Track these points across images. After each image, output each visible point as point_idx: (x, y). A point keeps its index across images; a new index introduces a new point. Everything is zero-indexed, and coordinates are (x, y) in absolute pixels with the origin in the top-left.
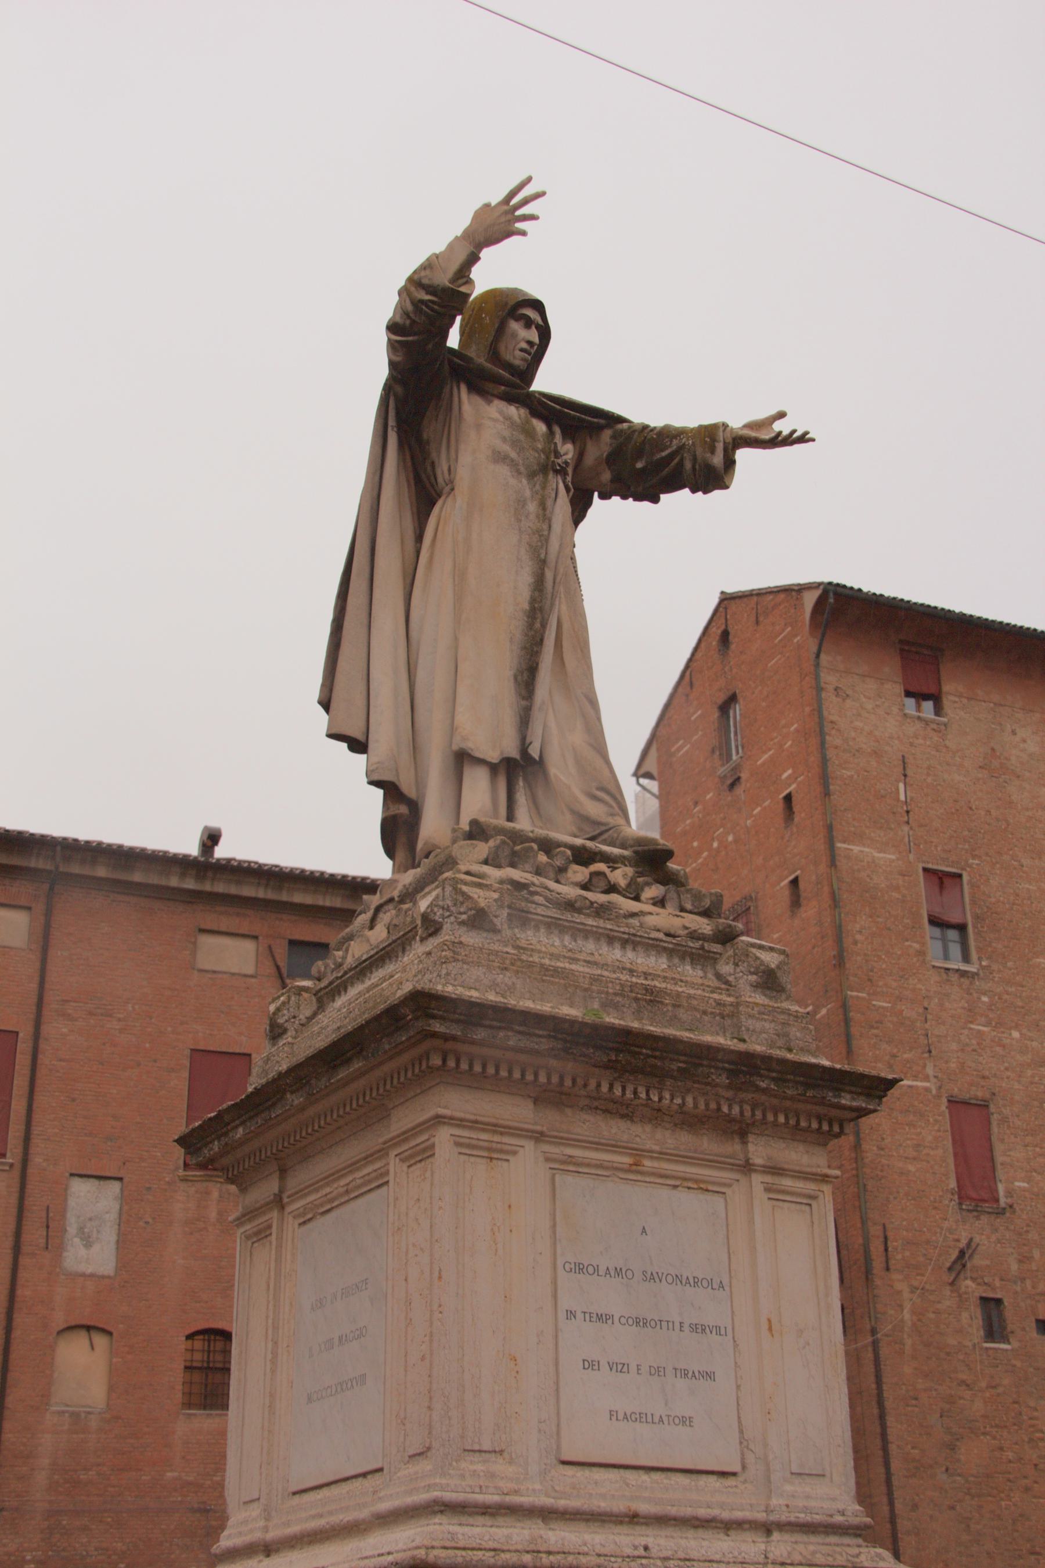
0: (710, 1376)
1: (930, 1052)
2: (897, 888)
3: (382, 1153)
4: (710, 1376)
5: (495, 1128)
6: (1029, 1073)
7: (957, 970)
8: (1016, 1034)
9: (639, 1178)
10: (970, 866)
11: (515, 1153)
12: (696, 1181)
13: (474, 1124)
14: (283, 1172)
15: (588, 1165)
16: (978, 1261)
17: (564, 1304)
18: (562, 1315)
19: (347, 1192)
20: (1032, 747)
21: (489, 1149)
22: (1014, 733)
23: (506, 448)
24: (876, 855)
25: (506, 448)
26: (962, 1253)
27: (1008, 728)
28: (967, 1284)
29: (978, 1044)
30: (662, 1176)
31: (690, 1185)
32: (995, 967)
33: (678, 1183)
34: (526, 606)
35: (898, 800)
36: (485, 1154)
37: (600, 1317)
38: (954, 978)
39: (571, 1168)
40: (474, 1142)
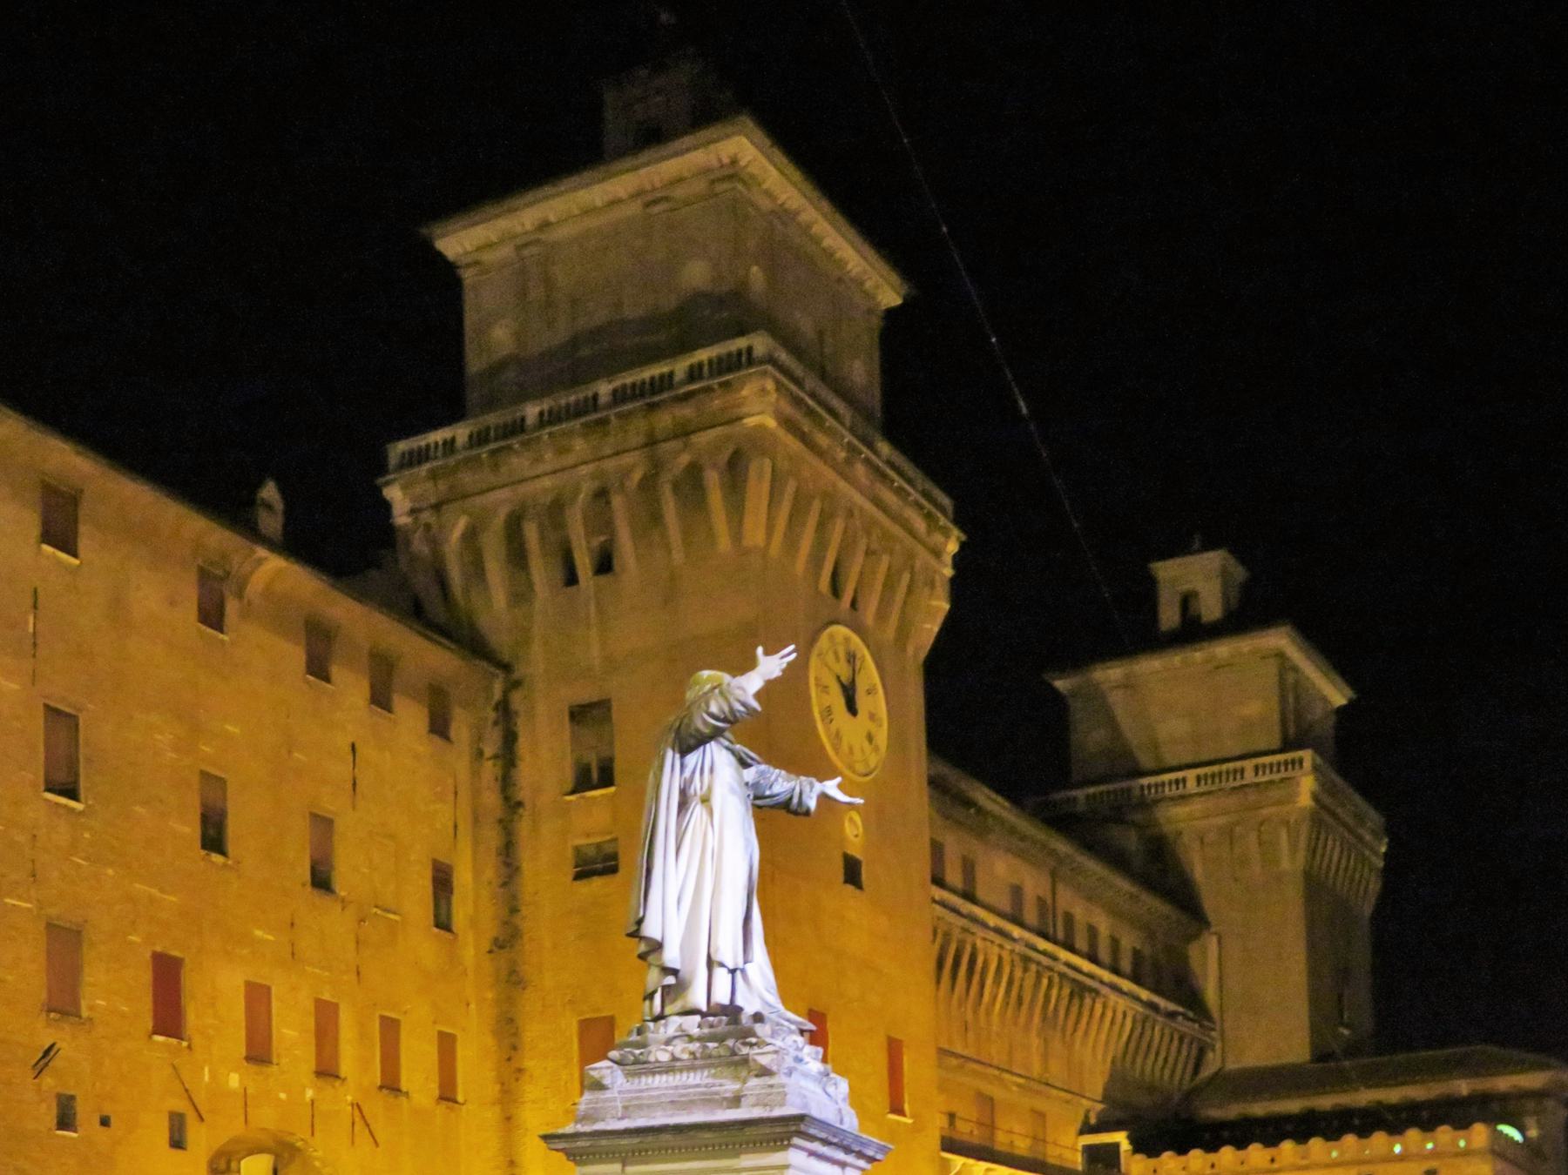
14: (624, 1165)
16: (57, 1063)
26: (47, 1053)
28: (48, 1081)
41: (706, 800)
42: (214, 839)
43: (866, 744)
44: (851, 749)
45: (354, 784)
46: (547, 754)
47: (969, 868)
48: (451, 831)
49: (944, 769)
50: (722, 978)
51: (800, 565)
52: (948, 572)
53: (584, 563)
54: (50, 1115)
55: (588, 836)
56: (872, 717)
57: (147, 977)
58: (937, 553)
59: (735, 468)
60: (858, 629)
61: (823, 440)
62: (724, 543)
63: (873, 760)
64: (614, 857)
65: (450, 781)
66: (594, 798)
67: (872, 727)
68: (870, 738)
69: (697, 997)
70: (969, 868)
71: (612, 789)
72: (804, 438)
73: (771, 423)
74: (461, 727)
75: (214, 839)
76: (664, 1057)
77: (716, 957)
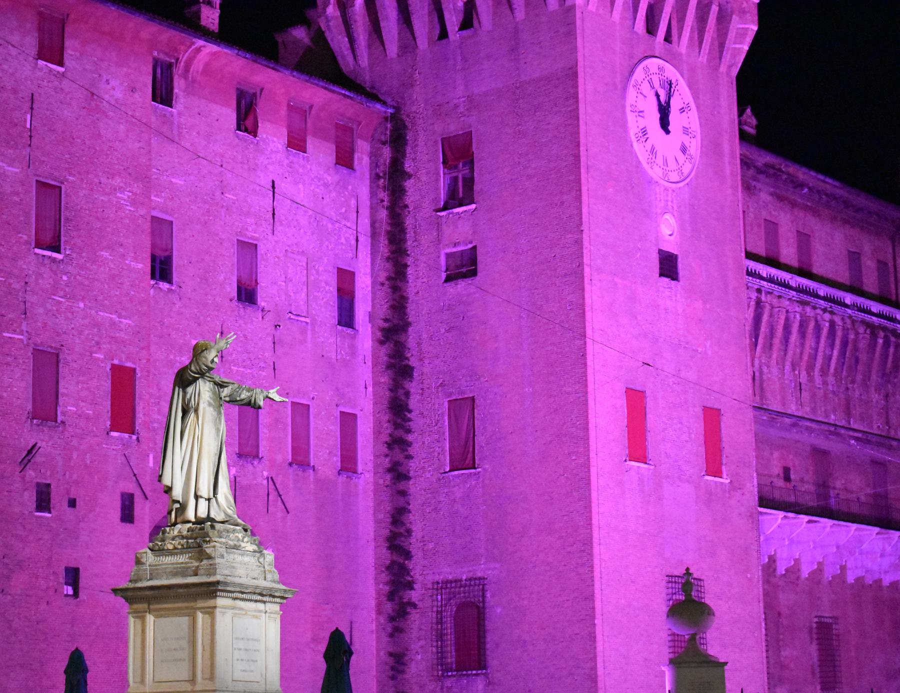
1: (25, 314)
2: (17, 194)
6: (86, 332)
7: (50, 257)
8: (81, 305)
10: (67, 180)
16: (39, 459)
20: (118, 94)
22: (108, 82)
24: (7, 168)
26: (30, 452)
27: (105, 77)
28: (30, 473)
29: (57, 310)
32: (74, 255)
35: (25, 127)
38: (46, 261)
41: (196, 411)
42: (161, 269)
43: (681, 157)
44: (666, 162)
45: (274, 214)
46: (427, 179)
48: (353, 242)
50: (203, 504)
51: (617, 15)
53: (453, 21)
54: (30, 498)
55: (455, 245)
56: (686, 131)
57: (106, 385)
60: (672, 59)
63: (687, 169)
65: (353, 202)
66: (458, 213)
67: (686, 139)
68: (684, 150)
69: (190, 515)
71: (473, 206)
74: (362, 159)
75: (161, 269)
76: (171, 547)
77: (199, 494)
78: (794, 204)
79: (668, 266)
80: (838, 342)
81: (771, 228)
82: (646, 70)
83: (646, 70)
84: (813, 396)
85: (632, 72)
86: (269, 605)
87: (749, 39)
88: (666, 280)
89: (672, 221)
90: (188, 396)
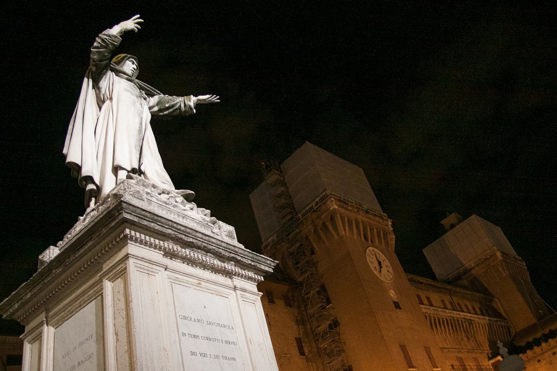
0: (234, 359)
3: (100, 281)
4: (234, 359)
5: (150, 262)
9: (200, 289)
11: (158, 273)
12: (219, 292)
13: (142, 259)
15: (183, 282)
17: (181, 330)
18: (181, 335)
19: (80, 306)
21: (148, 270)
23: (129, 89)
25: (129, 89)
30: (208, 289)
31: (217, 293)
33: (213, 292)
34: (138, 128)
36: (147, 272)
37: (194, 336)
39: (177, 282)
40: (142, 267)
41: (111, 99)
43: (389, 274)
47: (428, 299)
49: (411, 276)
51: (355, 236)
52: (391, 229)
56: (387, 266)
58: (387, 225)
59: (332, 219)
61: (351, 208)
62: (336, 237)
63: (391, 277)
64: (337, 322)
67: (388, 269)
68: (388, 271)
70: (428, 299)
72: (345, 208)
73: (336, 207)
78: (422, 289)
79: (397, 305)
80: (450, 324)
81: (419, 297)
82: (369, 250)
83: (369, 250)
84: (449, 341)
85: (366, 252)
86: (238, 282)
87: (394, 239)
88: (398, 310)
89: (393, 292)
90: (103, 91)
